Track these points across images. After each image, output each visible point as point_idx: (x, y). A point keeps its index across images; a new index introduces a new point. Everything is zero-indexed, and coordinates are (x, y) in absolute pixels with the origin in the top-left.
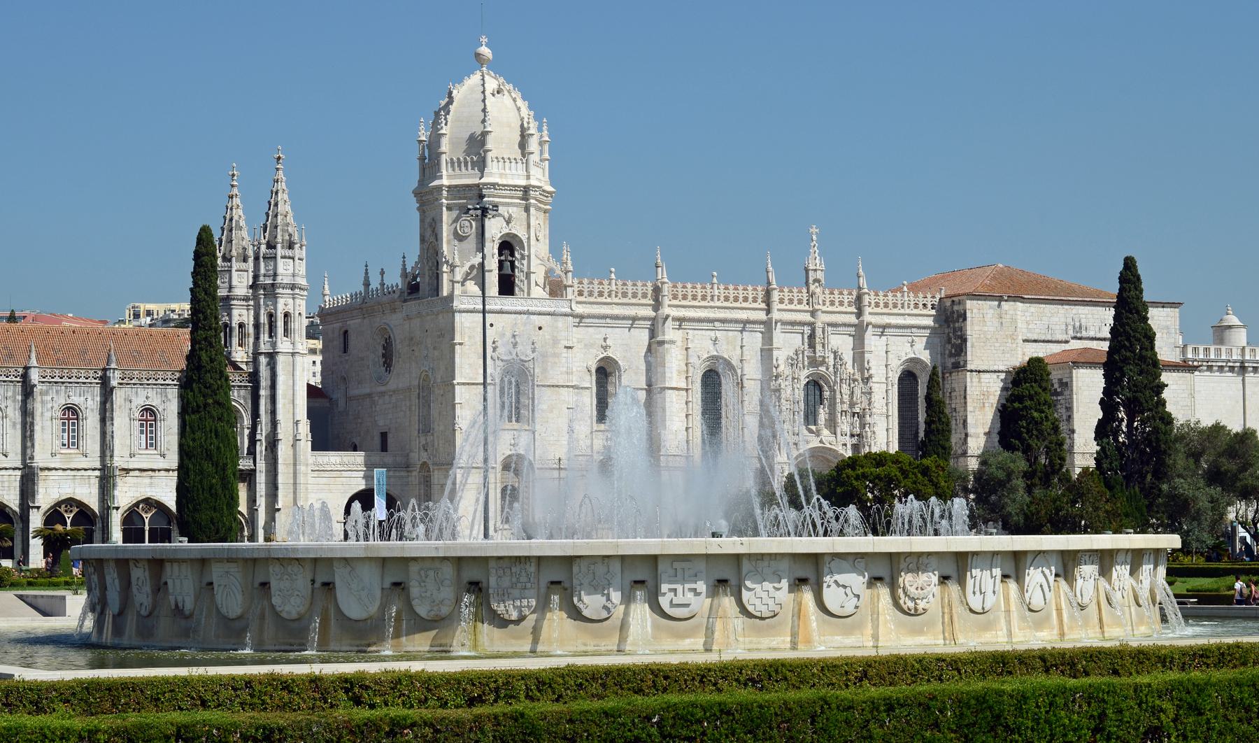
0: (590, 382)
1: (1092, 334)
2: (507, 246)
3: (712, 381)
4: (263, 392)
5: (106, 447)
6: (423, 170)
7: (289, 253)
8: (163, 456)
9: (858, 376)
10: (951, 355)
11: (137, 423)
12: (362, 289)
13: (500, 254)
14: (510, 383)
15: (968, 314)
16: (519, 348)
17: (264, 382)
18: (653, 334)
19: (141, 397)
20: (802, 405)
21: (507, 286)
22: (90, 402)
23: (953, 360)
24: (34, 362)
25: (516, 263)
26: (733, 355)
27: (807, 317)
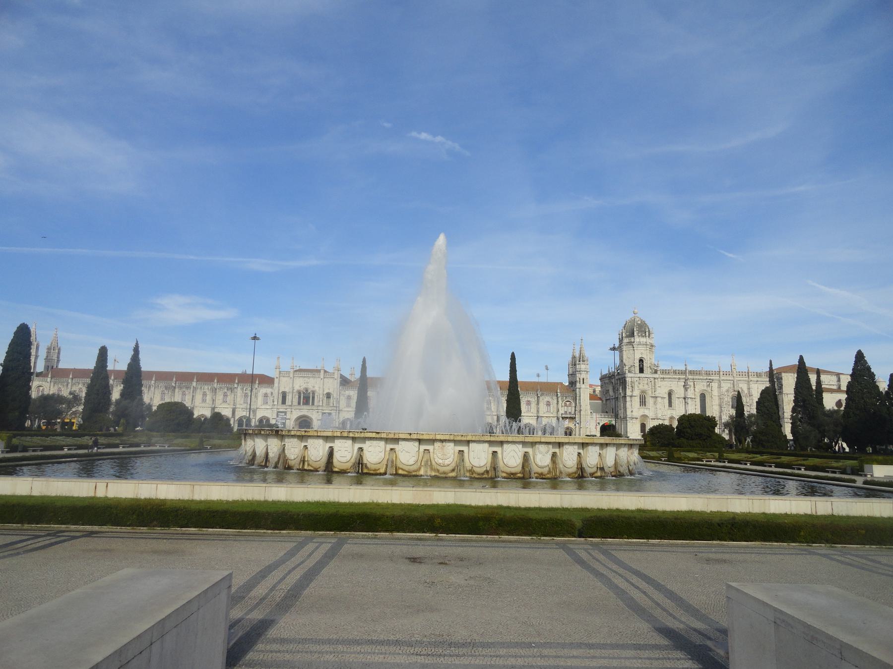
0: (666, 396)
1: (826, 383)
2: (641, 361)
3: (703, 397)
4: (577, 398)
5: (538, 411)
6: (620, 342)
7: (583, 363)
8: (552, 413)
9: (748, 395)
10: (779, 389)
12: (608, 372)
13: (639, 362)
15: (783, 378)
16: (645, 387)
17: (577, 396)
18: (685, 383)
19: (547, 399)
21: (641, 370)
22: (533, 400)
26: (709, 389)
27: (732, 378)
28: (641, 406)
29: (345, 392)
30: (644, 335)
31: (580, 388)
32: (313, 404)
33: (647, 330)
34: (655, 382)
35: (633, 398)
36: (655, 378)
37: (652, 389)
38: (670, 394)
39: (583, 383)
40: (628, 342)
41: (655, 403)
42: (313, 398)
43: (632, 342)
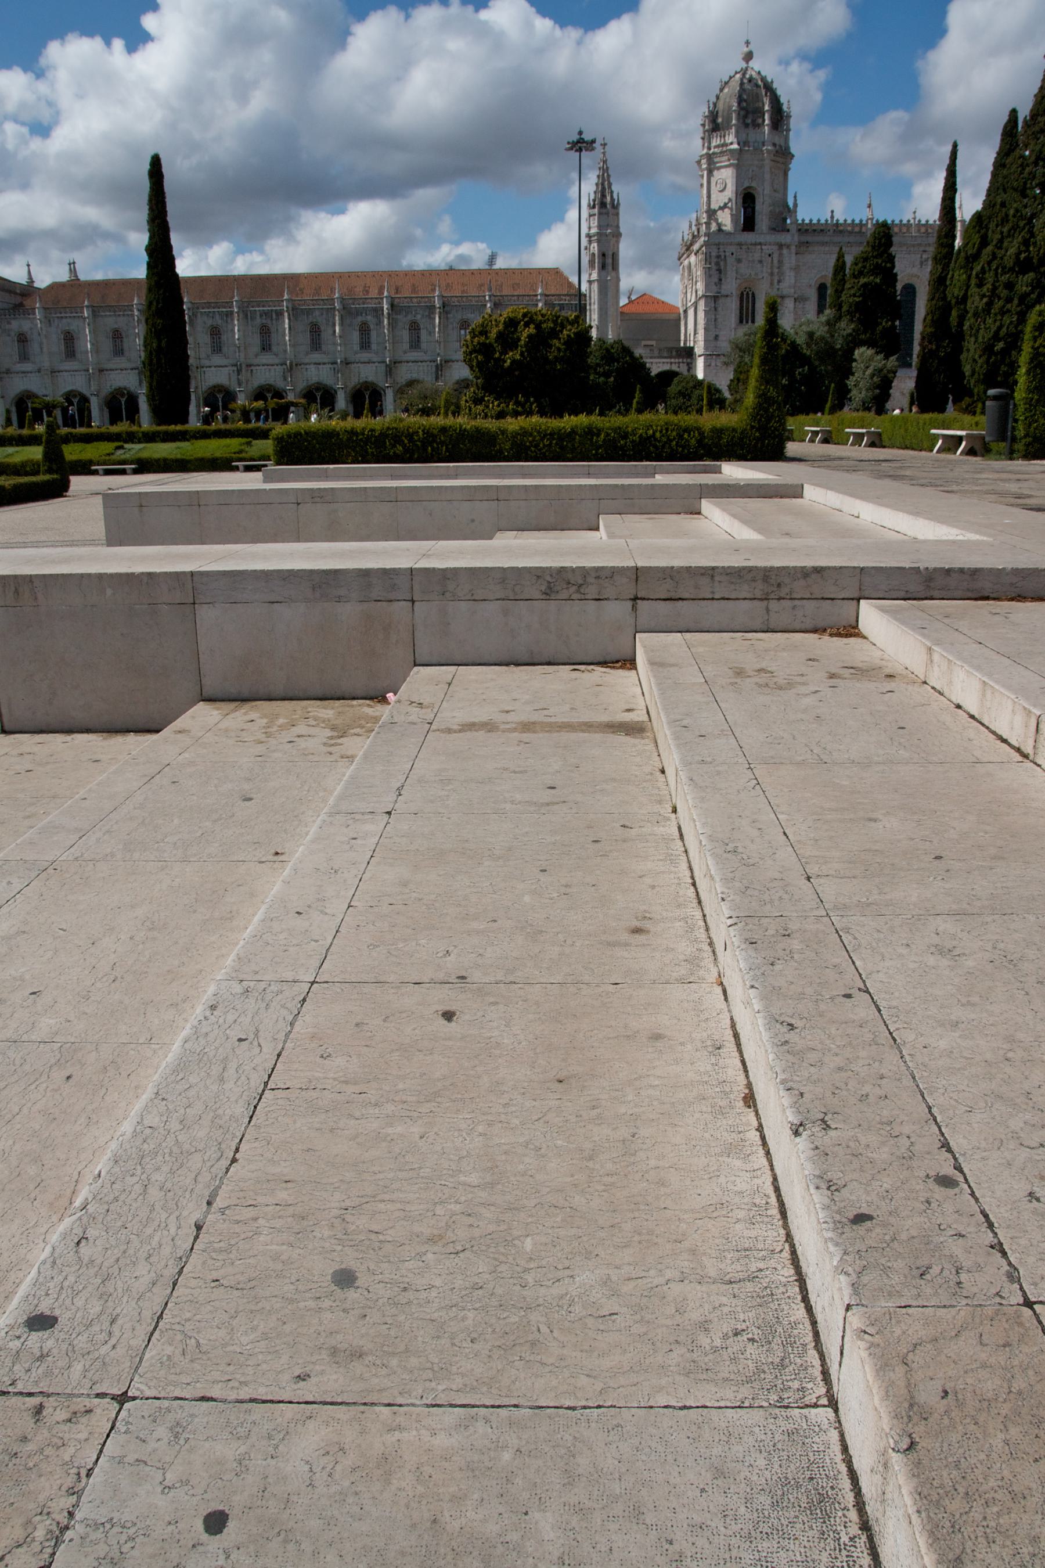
14: (748, 294)
21: (749, 224)
24: (437, 293)
25: (757, 208)
28: (741, 321)
29: (9, 323)
34: (781, 255)
35: (721, 301)
36: (781, 246)
37: (772, 274)
43: (727, 145)
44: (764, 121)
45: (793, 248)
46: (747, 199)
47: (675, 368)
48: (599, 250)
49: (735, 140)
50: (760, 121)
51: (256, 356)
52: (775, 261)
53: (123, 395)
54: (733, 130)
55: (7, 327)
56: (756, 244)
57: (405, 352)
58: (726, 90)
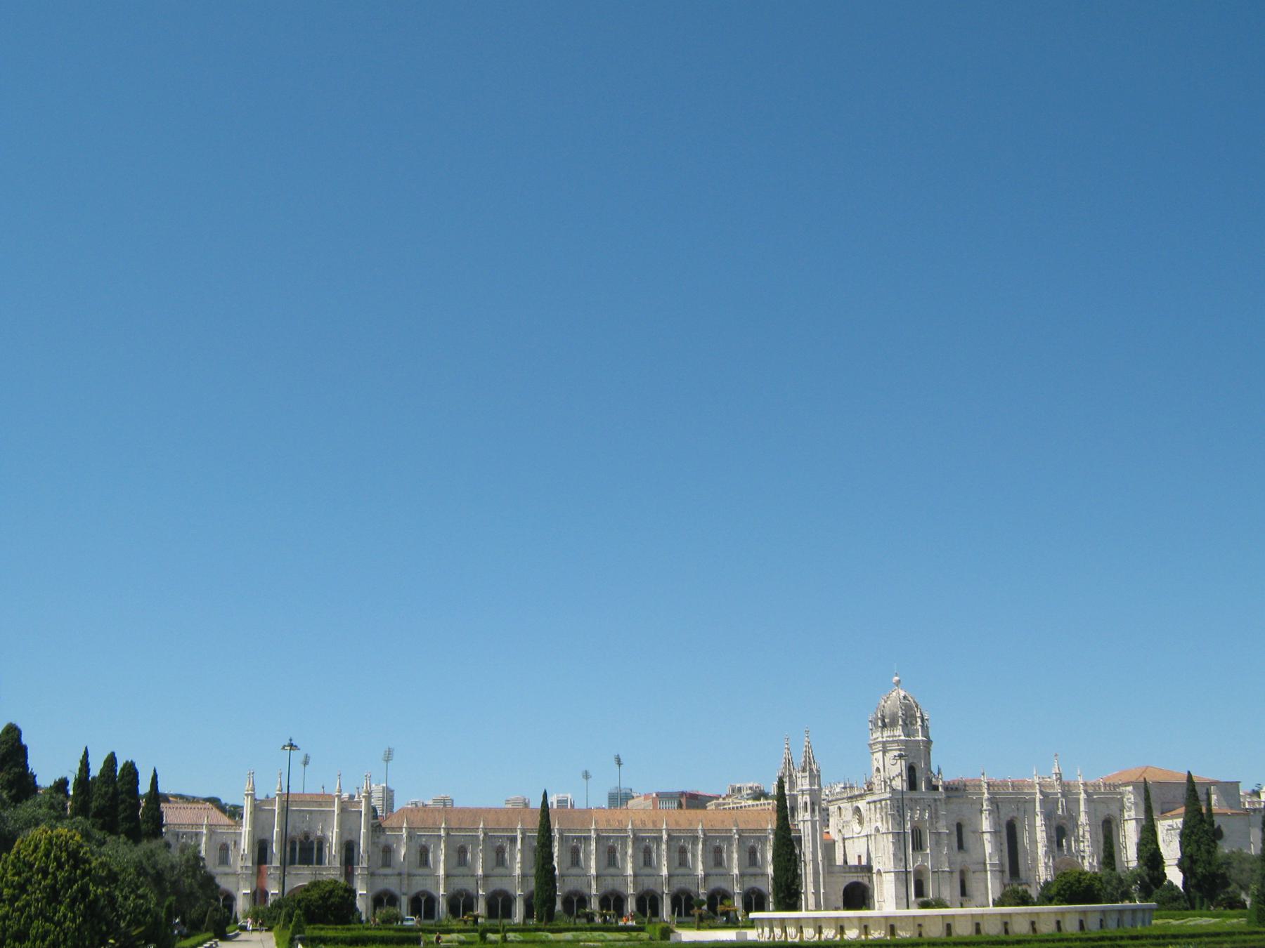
0: (955, 829)
4: (803, 838)
10: (1127, 811)
11: (748, 854)
13: (909, 772)
14: (916, 831)
20: (1056, 838)
21: (913, 785)
23: (1128, 813)
28: (913, 849)
30: (914, 722)
31: (807, 821)
32: (320, 861)
33: (918, 715)
36: (935, 800)
38: (959, 827)
39: (813, 811)
40: (889, 737)
41: (937, 843)
42: (320, 850)
43: (896, 736)
44: (917, 722)
45: (943, 801)
46: (911, 770)
47: (860, 880)
48: (810, 801)
49: (902, 734)
50: (914, 722)
51: (568, 869)
52: (933, 809)
53: (462, 896)
54: (900, 727)
55: (376, 840)
56: (920, 799)
57: (676, 869)
58: (889, 702)
